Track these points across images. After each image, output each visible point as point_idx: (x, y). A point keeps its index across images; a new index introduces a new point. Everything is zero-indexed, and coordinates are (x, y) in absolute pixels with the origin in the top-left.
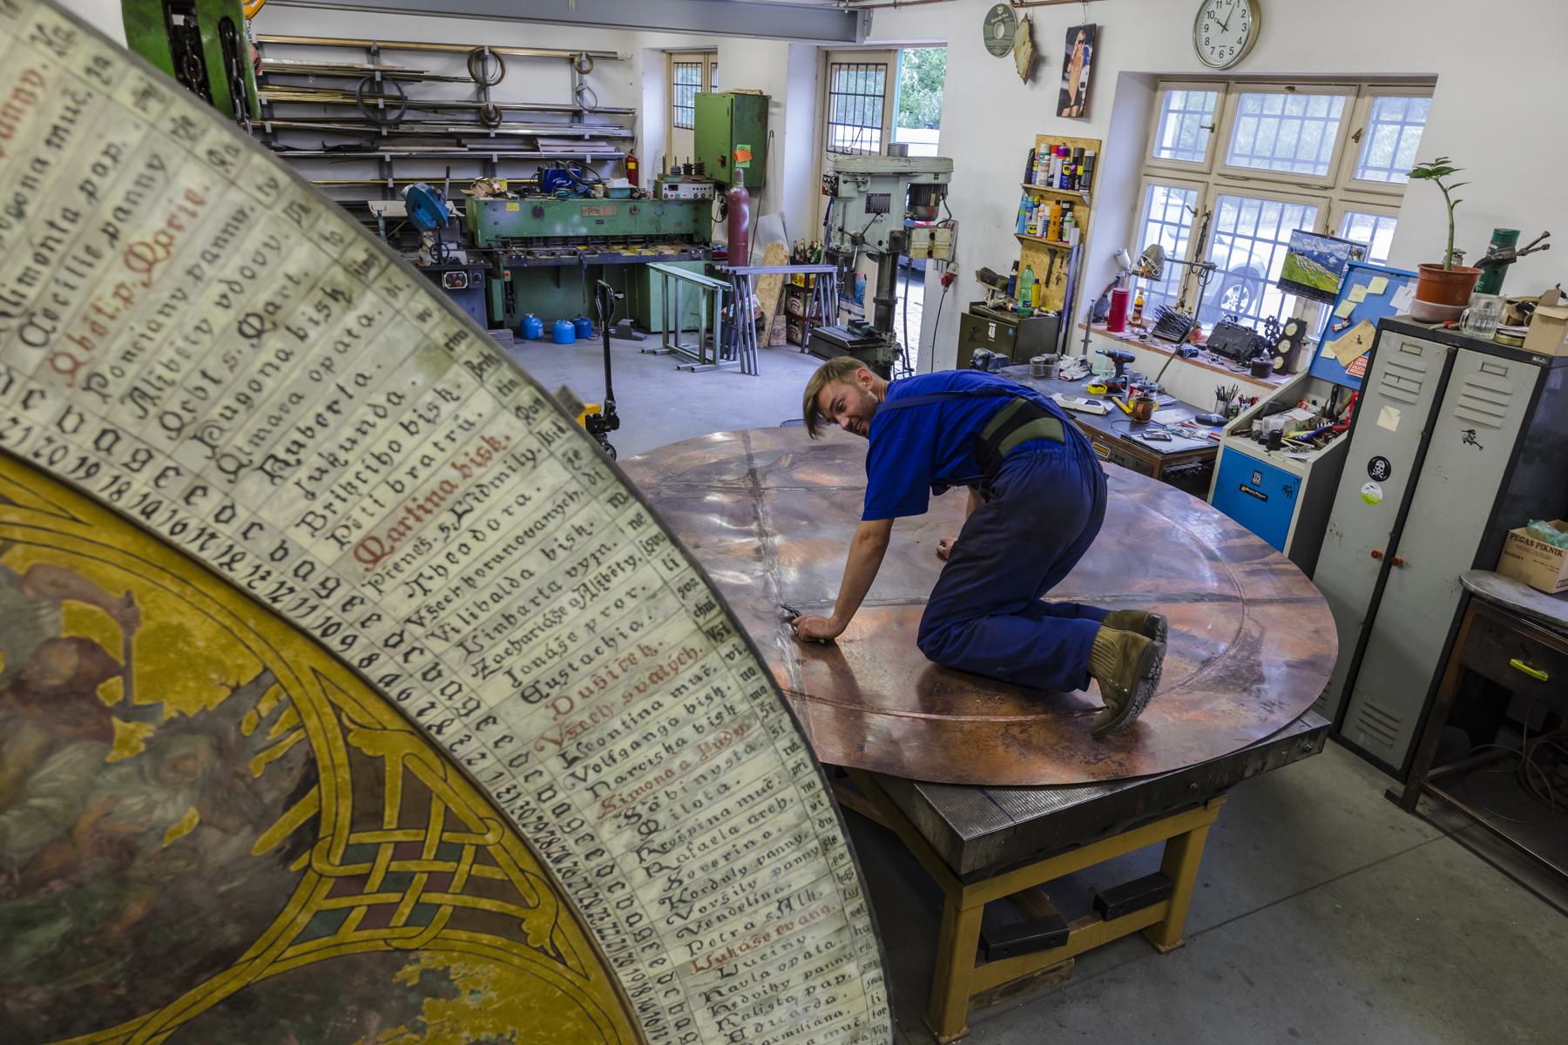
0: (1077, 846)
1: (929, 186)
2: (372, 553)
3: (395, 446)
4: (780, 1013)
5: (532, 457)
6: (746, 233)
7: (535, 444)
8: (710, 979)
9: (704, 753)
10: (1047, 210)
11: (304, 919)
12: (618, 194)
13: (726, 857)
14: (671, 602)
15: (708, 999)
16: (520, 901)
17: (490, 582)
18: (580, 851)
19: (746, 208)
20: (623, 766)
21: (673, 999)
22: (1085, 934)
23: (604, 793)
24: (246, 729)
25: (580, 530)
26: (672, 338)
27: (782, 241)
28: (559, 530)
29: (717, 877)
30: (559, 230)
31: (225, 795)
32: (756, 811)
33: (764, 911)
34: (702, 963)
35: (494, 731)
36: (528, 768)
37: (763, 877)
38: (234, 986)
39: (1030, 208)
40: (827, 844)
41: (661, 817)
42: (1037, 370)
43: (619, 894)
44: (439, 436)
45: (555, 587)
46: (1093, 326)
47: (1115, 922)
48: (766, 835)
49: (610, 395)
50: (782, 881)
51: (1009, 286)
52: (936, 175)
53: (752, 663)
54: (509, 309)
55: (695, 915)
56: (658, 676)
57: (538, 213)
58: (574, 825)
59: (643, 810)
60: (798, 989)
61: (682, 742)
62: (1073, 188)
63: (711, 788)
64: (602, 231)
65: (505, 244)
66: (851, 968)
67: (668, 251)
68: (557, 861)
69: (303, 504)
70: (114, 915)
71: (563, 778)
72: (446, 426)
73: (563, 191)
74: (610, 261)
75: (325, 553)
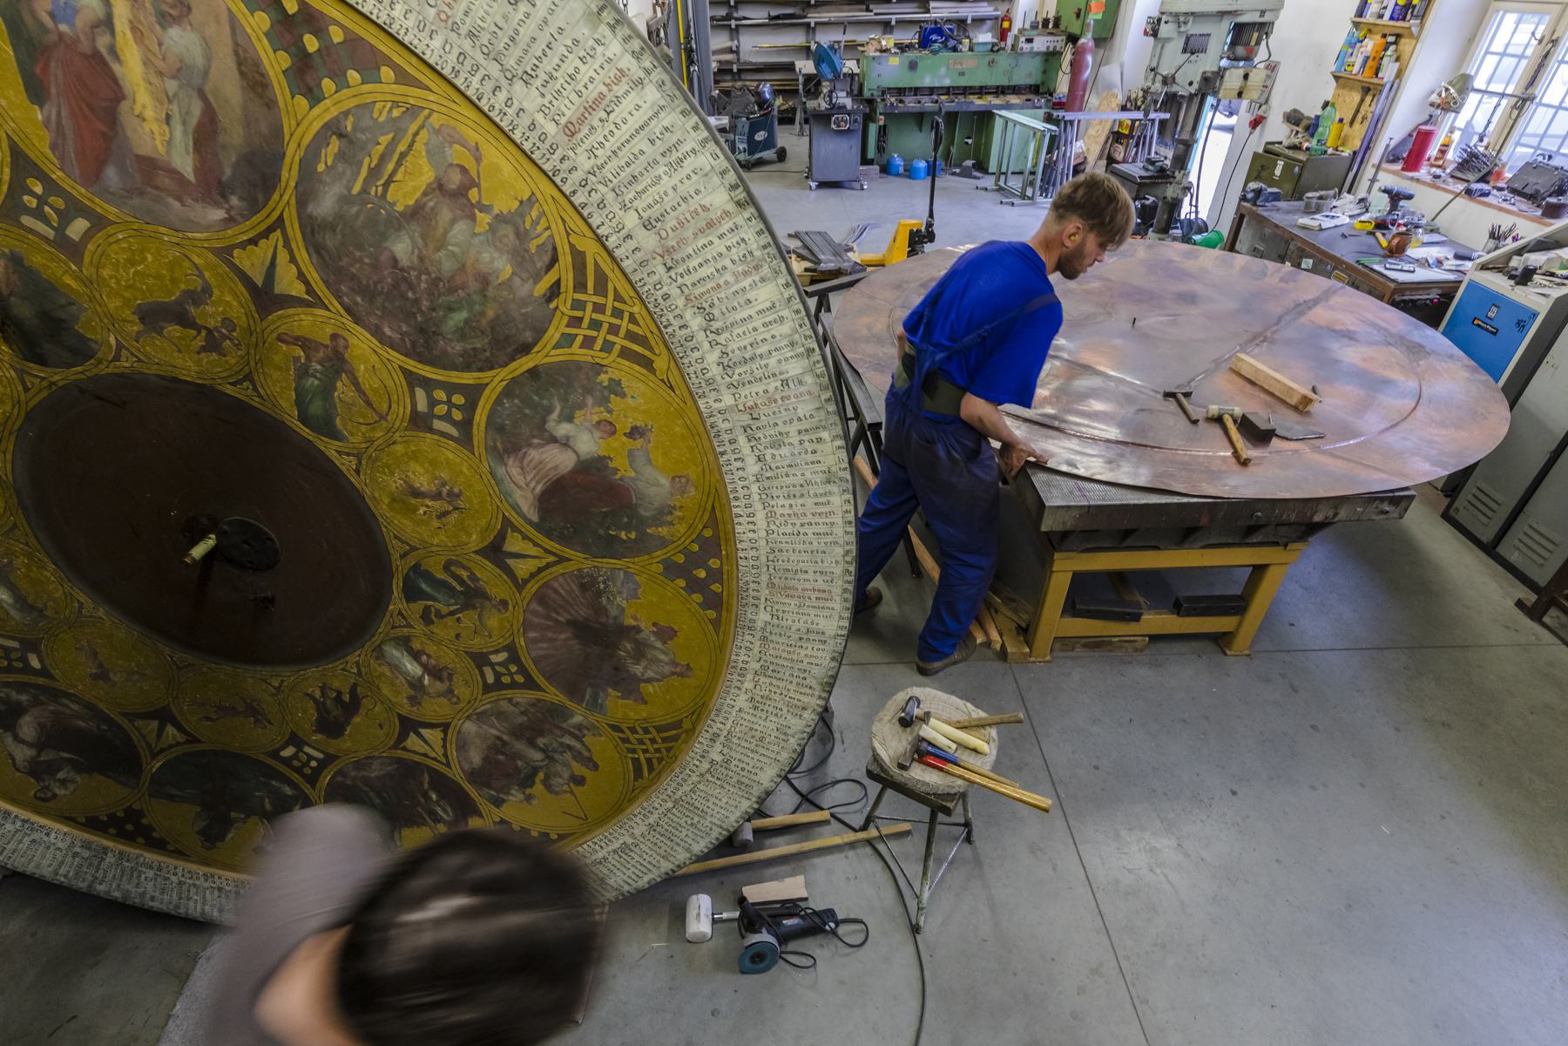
0: (1156, 548)
1: (1254, 24)
2: (570, 131)
3: (577, 70)
4: (785, 451)
5: (640, 82)
6: (1086, 83)
7: (642, 75)
8: (745, 419)
10: (1370, 45)
11: (557, 336)
12: (981, 48)
14: (716, 179)
16: (651, 349)
17: (625, 154)
18: (676, 323)
19: (1089, 58)
20: (695, 277)
22: (1157, 621)
23: (686, 291)
24: (528, 225)
25: (667, 129)
26: (1003, 178)
27: (1118, 91)
28: (656, 127)
30: (927, 82)
31: (520, 257)
32: (767, 320)
33: (773, 385)
35: (632, 244)
36: (649, 269)
37: (772, 361)
38: (531, 365)
39: (1353, 43)
40: (810, 351)
41: (716, 312)
42: (1308, 206)
43: (696, 354)
44: (596, 66)
45: (656, 162)
46: (1385, 165)
47: (1188, 620)
48: (773, 337)
49: (931, 215)
51: (1312, 127)
52: (1263, 13)
53: (762, 226)
54: (880, 149)
55: (736, 377)
56: (710, 225)
57: (913, 66)
59: (706, 305)
60: (795, 439)
61: (725, 268)
62: (1404, 19)
64: (963, 82)
65: (883, 93)
66: (825, 435)
67: (1014, 99)
69: (540, 100)
70: (483, 314)
71: (666, 280)
72: (600, 60)
73: (936, 46)
74: (964, 108)
75: (551, 128)
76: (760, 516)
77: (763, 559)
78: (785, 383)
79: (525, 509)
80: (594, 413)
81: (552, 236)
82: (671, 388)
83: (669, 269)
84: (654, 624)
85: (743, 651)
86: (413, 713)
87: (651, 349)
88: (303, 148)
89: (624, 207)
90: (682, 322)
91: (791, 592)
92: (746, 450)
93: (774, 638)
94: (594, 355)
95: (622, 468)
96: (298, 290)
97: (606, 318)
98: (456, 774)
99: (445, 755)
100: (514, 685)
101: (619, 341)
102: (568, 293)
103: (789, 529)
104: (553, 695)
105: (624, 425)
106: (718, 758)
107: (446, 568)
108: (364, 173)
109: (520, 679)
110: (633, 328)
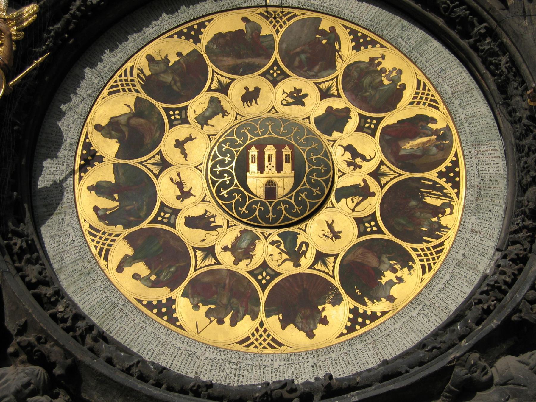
16: (429, 271)
18: (443, 273)
21: (422, 300)
35: (456, 254)
41: (454, 281)
43: (438, 282)
56: (474, 269)
76: (399, 324)
77: (383, 334)
79: (347, 259)
80: (397, 267)
82: (421, 282)
83: (456, 265)
84: (325, 317)
85: (338, 349)
86: (218, 251)
87: (429, 271)
89: (464, 249)
91: (376, 349)
92: (418, 309)
93: (352, 355)
94: (417, 259)
95: (384, 280)
98: (192, 274)
99: (201, 268)
102: (430, 245)
103: (400, 335)
104: (263, 297)
105: (399, 274)
106: (276, 366)
107: (302, 243)
108: (428, 191)
109: (264, 282)
110: (432, 265)
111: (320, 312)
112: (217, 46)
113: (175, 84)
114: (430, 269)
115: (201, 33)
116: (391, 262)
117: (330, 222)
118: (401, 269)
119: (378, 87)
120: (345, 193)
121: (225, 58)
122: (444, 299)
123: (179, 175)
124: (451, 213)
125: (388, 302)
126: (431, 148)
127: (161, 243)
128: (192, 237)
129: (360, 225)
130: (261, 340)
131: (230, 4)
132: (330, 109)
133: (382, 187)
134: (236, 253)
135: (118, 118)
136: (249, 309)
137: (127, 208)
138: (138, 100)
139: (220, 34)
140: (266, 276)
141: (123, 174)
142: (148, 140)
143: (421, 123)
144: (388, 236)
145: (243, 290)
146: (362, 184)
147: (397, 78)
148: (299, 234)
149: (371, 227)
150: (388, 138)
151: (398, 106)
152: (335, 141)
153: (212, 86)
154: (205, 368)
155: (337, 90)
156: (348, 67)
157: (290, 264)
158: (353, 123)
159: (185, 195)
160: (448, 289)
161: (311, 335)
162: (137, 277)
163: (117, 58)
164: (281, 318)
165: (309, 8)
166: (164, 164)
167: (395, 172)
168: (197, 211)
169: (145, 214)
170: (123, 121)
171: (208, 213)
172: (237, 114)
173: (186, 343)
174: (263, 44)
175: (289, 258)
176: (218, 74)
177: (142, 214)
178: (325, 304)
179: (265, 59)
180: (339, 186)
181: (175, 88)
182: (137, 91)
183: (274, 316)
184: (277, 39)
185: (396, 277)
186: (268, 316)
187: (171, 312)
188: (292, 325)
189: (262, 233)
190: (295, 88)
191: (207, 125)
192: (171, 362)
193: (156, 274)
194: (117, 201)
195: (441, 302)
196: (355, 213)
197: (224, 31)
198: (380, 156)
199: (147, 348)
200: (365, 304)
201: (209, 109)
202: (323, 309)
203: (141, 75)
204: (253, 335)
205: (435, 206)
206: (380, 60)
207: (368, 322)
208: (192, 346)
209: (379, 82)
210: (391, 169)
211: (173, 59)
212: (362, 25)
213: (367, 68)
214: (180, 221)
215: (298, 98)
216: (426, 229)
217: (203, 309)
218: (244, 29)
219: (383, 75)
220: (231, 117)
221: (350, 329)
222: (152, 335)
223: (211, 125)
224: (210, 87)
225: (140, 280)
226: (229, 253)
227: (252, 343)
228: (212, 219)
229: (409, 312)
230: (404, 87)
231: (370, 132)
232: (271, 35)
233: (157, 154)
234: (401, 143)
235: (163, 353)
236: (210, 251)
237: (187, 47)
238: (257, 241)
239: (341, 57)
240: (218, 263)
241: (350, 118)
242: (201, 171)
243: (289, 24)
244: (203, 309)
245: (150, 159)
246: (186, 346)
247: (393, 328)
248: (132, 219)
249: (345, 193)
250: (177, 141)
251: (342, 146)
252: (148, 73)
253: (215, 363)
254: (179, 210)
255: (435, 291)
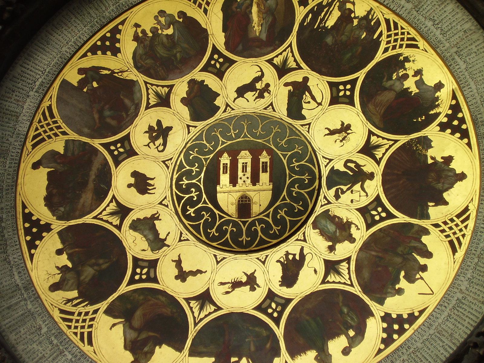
9: (439, 5)
13: (450, 24)
15: (456, 54)
16: (417, 41)
20: (426, 11)
21: (449, 54)
23: (424, 16)
29: (450, 28)
34: (452, 46)
35: (404, 9)
37: (459, 27)
41: (435, 18)
43: (432, 34)
50: (463, 28)
55: (448, 36)
58: (421, 22)
63: (443, 12)
68: (420, 29)
71: (417, 15)
77: (479, 102)
78: (465, 32)
79: (377, 123)
80: (401, 73)
81: (378, 18)
82: (426, 51)
86: (332, 257)
87: (417, 41)
88: (291, 35)
90: (425, 26)
94: (398, 51)
95: (414, 90)
96: (294, 65)
97: (400, 36)
98: (357, 290)
99: (350, 278)
100: (382, 219)
101: (405, 43)
104: (401, 218)
105: (411, 73)
107: (345, 165)
109: (384, 215)
110: (409, 36)
111: (436, 163)
112: (62, 206)
113: (99, 265)
114: (413, 39)
115: (38, 220)
116: (394, 78)
117: (328, 132)
118: (405, 69)
119: (173, 42)
120: (295, 109)
121: (82, 201)
122: (455, 32)
123: (222, 284)
124: (353, 3)
125: (442, 90)
126: (267, 5)
127: (308, 318)
128: (309, 282)
129: (340, 101)
130: (456, 229)
131: (9, 177)
132: (183, 101)
133: (300, 68)
134: (340, 238)
135: (128, 340)
136: (414, 236)
137: (253, 348)
138: (109, 312)
139: (46, 199)
140: (377, 211)
141: (205, 347)
142: (167, 311)
143: (234, 7)
144: (361, 75)
145: (389, 239)
146: (290, 88)
147: (168, 18)
148: (333, 167)
149: (345, 90)
150: (240, 47)
151: (204, 26)
152: (227, 105)
153: (114, 223)
154: (478, 293)
155: (163, 86)
156: (136, 67)
157: (368, 183)
158: (211, 81)
159: (251, 281)
160: (443, 27)
161: (462, 177)
162: (347, 350)
163: (43, 326)
164: (434, 204)
165: (45, 89)
166: (205, 298)
167: (285, 50)
168: (277, 272)
169: (265, 330)
170: (133, 335)
171: (282, 260)
172: (161, 203)
173: (444, 308)
174: (76, 153)
175: (360, 183)
176: (101, 213)
177: (265, 333)
178: (427, 156)
179: (96, 155)
180: (286, 113)
181: (104, 267)
182: (95, 312)
183: (429, 211)
184: (73, 136)
185: (413, 76)
186: (428, 217)
187: (400, 320)
188: (445, 195)
189: (322, 206)
190: (146, 132)
191: (165, 239)
192: (464, 328)
193: (348, 329)
194: (240, 359)
195: (457, 36)
196: (323, 103)
197: (44, 193)
198: (262, 61)
199: (442, 351)
200: (437, 115)
201: (145, 233)
202: (432, 158)
203: (75, 302)
204: (447, 236)
205: (339, 18)
206: (139, 30)
207: (460, 115)
208: (449, 302)
209: (167, 39)
210: (281, 54)
211: (64, 260)
212: (88, 37)
213: (144, 47)
214: (284, 292)
215: (159, 133)
216: (365, 34)
217: (403, 283)
218: (49, 170)
219: (160, 32)
220: (162, 210)
221: (465, 134)
222: (427, 343)
223: (168, 235)
224: (116, 226)
225: (352, 347)
226: (338, 246)
227: (458, 239)
228: (291, 257)
229: (459, 70)
230: (182, 14)
231: (227, 65)
232: (67, 142)
233: (189, 304)
234: (251, 35)
235: (451, 335)
236: (331, 267)
237: (51, 242)
238: (330, 213)
239: (122, 72)
240: (348, 260)
241: (203, 81)
242: (224, 258)
243: (58, 118)
244: (403, 283)
245: (193, 313)
246: (448, 310)
247: (475, 91)
248: (268, 346)
249: (295, 109)
250: (177, 278)
251: (235, 99)
252: (74, 294)
253: (474, 280)
254: (270, 291)
255: (442, 39)
